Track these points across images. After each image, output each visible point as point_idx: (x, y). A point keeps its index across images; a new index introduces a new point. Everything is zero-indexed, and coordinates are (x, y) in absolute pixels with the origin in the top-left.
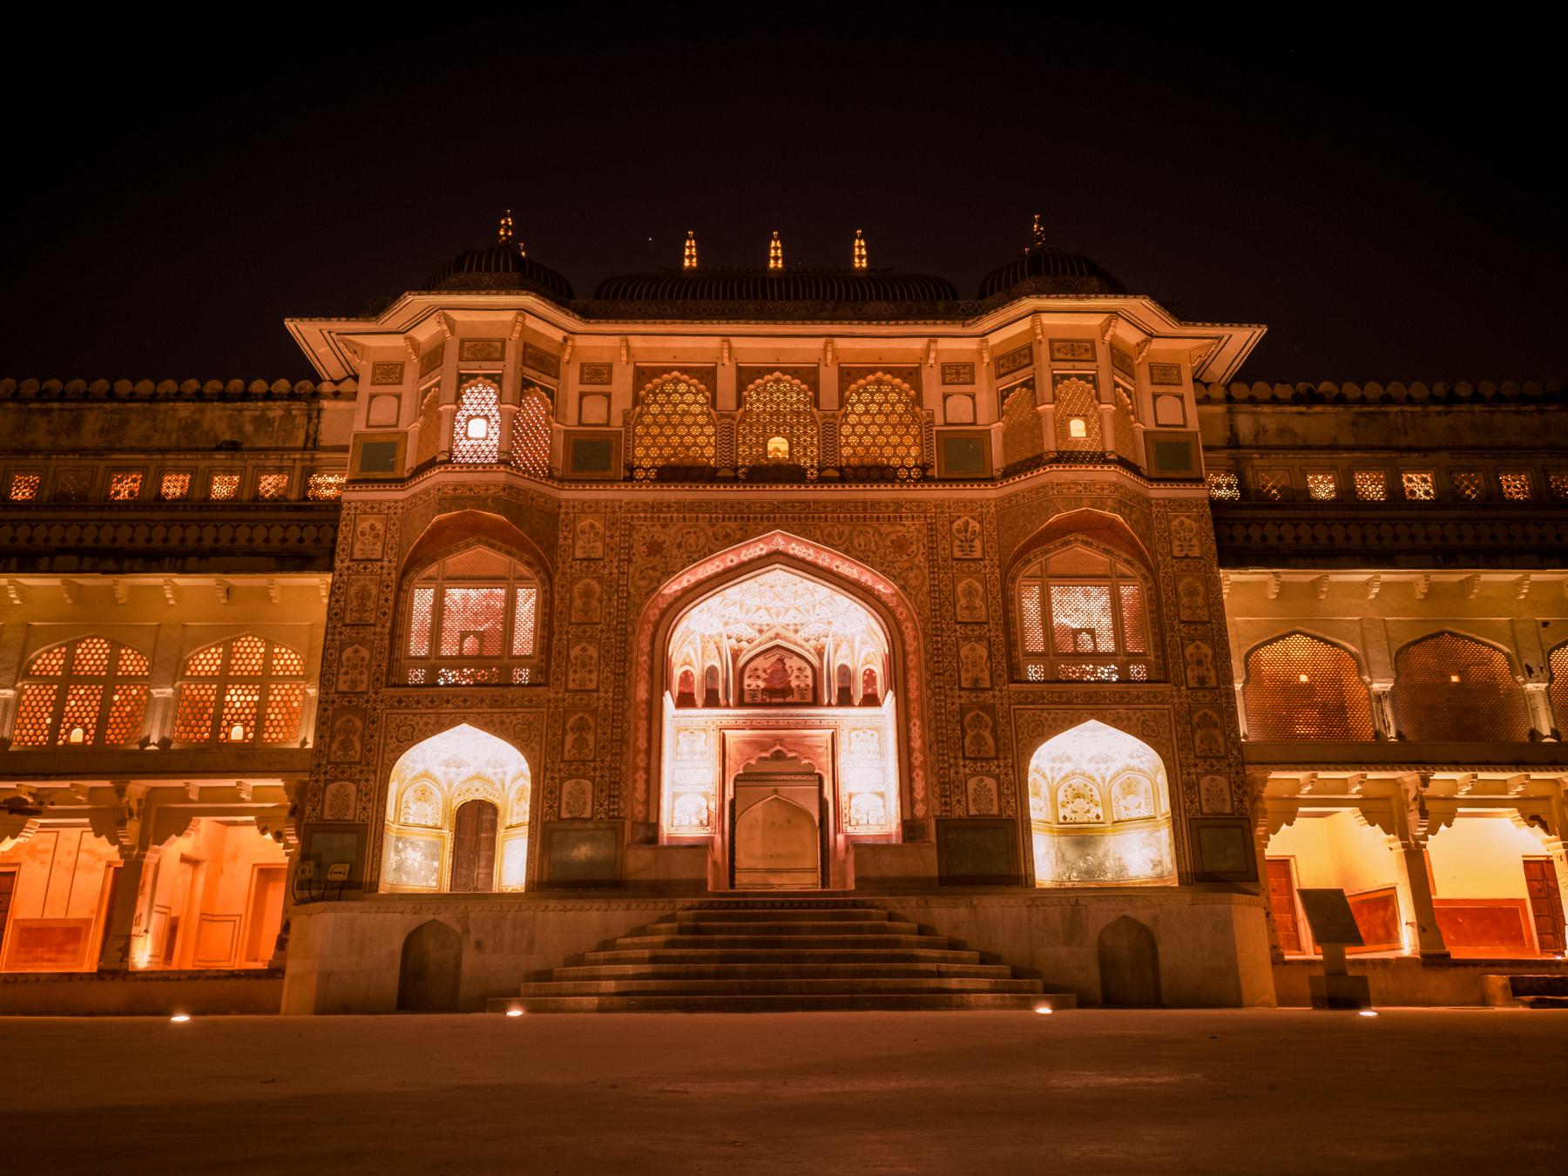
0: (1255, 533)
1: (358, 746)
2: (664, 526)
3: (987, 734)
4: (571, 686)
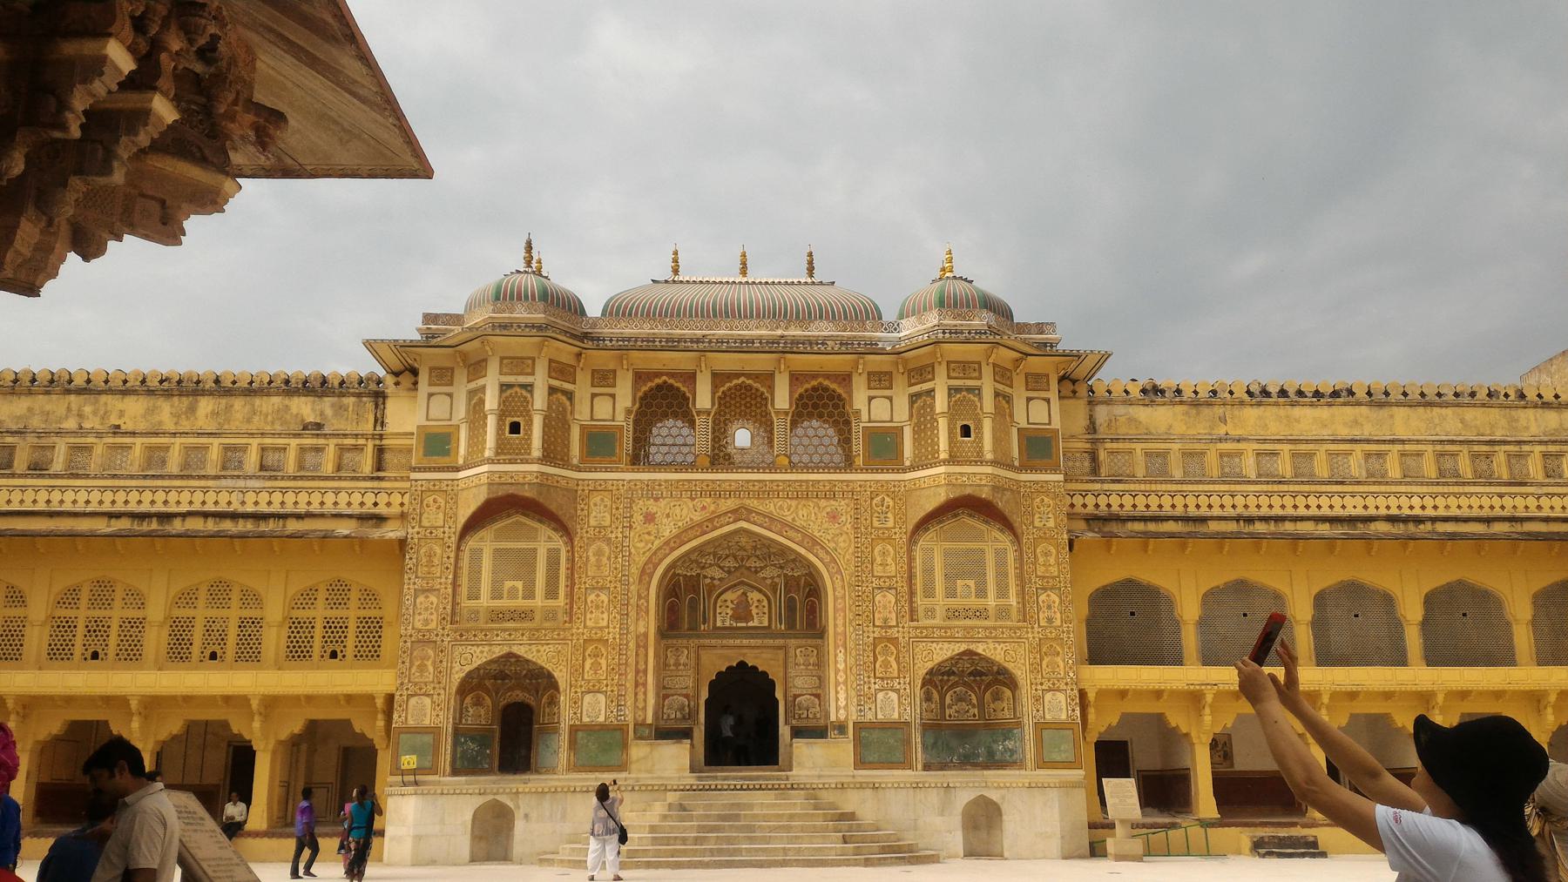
0: (1102, 501)
1: (431, 669)
2: (656, 499)
3: (892, 659)
4: (589, 623)
